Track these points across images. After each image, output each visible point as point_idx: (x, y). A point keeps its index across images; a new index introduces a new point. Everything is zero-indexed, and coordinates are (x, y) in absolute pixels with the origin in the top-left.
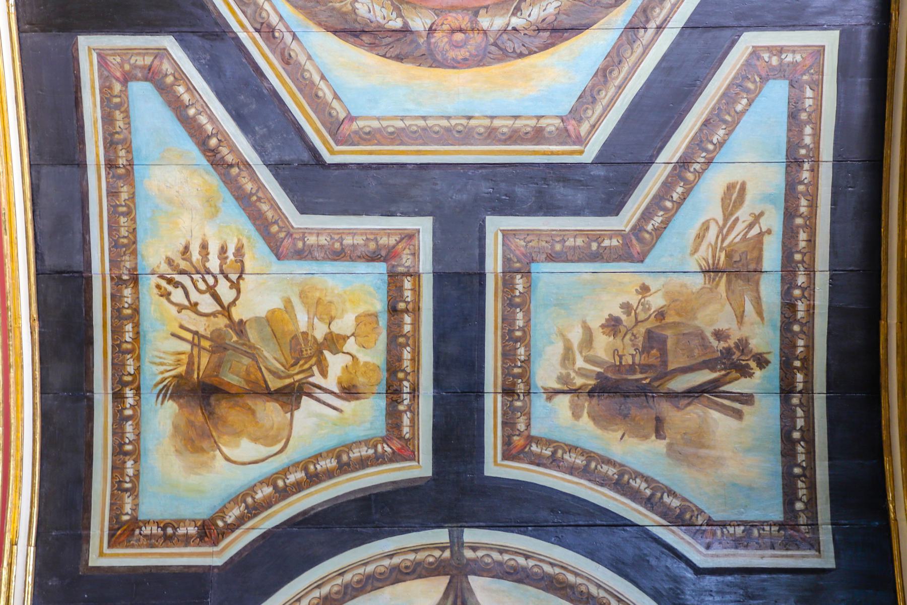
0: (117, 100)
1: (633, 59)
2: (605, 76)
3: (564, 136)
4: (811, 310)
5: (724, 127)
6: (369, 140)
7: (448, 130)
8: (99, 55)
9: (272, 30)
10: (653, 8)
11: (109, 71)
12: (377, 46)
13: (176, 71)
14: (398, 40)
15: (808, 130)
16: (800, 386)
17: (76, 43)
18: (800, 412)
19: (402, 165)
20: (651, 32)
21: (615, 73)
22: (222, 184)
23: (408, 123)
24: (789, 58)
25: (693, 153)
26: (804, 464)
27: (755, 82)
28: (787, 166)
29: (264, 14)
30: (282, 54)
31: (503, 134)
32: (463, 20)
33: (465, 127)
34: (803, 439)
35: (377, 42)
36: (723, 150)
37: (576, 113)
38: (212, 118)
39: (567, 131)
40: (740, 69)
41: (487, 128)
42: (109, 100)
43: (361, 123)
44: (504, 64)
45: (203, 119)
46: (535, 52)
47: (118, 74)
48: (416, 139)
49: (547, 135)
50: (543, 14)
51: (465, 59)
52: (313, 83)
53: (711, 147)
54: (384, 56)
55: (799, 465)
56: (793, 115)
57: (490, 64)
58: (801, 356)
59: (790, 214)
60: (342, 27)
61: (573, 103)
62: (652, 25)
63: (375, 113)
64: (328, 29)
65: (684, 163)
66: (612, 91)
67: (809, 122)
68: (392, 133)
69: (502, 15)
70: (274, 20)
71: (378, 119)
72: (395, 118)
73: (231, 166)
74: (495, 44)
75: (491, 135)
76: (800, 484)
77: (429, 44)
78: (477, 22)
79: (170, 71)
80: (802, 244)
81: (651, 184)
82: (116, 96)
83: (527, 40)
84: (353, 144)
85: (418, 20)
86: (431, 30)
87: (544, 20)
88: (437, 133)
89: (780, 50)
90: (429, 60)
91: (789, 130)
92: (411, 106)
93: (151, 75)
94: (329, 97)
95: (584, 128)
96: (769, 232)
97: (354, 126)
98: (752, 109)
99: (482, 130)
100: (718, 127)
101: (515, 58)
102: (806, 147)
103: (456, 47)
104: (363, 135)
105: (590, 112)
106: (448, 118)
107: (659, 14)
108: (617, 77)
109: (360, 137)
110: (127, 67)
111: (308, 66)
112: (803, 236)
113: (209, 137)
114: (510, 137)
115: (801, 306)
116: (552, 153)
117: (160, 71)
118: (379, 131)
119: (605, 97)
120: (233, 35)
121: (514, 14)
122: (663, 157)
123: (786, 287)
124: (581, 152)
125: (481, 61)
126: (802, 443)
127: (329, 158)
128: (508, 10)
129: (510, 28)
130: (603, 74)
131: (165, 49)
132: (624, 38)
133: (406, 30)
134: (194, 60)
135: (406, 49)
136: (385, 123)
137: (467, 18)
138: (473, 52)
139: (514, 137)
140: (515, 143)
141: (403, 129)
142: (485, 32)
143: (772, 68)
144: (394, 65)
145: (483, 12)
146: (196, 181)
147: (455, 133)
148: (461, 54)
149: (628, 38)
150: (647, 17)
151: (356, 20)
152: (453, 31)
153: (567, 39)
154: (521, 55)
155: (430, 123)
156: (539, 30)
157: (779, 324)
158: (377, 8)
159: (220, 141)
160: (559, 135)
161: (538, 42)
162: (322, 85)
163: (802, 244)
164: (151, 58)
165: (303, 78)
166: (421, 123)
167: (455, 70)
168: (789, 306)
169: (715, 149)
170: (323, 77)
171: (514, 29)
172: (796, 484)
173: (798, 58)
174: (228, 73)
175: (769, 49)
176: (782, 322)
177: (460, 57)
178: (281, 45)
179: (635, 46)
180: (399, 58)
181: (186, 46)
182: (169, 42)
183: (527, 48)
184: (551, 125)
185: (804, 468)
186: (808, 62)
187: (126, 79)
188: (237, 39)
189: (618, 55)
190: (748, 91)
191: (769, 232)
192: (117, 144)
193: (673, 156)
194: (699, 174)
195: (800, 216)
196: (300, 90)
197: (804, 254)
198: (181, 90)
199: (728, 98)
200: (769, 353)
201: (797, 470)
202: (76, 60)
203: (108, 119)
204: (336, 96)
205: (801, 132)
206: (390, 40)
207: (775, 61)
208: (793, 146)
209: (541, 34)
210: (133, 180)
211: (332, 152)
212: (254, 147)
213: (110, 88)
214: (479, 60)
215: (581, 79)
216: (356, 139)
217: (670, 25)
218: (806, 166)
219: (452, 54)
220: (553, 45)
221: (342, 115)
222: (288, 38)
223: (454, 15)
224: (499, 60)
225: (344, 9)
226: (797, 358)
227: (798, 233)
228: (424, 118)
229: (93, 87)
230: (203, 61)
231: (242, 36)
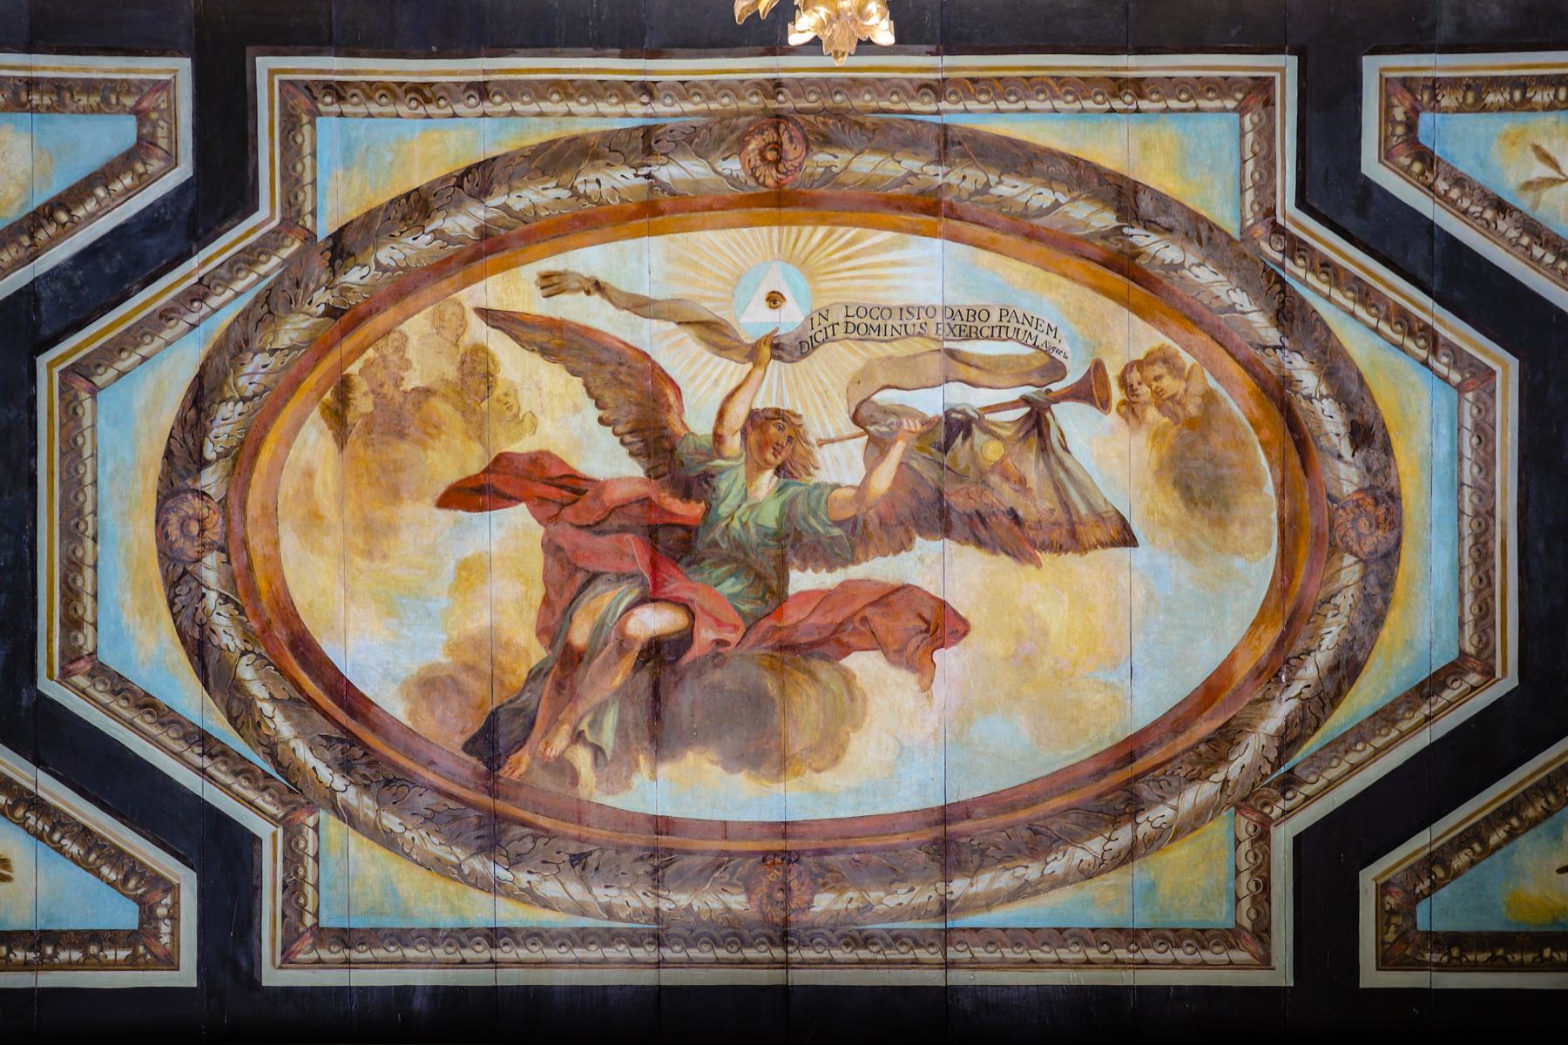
0: (113, 100)
1: (165, 739)
2: (146, 706)
3: (71, 656)
5: (82, 852)
6: (66, 413)
7: (80, 512)
8: (168, 82)
9: (202, 299)
10: (225, 763)
11: (149, 93)
12: (183, 428)
13: (151, 176)
14: (191, 455)
15: (76, 955)
17: (182, 55)
19: (33, 453)
20: (198, 761)
21: (148, 718)
22: (8, 223)
23: (88, 462)
24: (165, 928)
25: (48, 815)
27: (137, 888)
29: (219, 290)
30: (172, 310)
31: (74, 580)
32: (214, 533)
33: (83, 533)
35: (188, 428)
36: (53, 852)
37: (99, 671)
38: (92, 217)
39: (79, 658)
40: (153, 870)
41: (82, 560)
42: (113, 90)
43: (88, 404)
44: (161, 582)
45: (91, 206)
46: (175, 621)
47: (145, 104)
48: (68, 472)
49: (73, 634)
50: (220, 630)
51: (167, 536)
52: (137, 346)
53: (56, 837)
54: (171, 436)
56: (95, 936)
57: (161, 565)
60: (206, 385)
61: (113, 667)
62: (205, 762)
63: (101, 423)
64: (203, 367)
65: (37, 805)
66: (127, 714)
67: (87, 955)
68: (75, 441)
69: (219, 581)
70: (214, 302)
71: (93, 426)
72: (95, 447)
73: (32, 237)
74: (185, 572)
75: (72, 565)
77: (185, 492)
78: (211, 550)
79: (150, 169)
81: (10, 764)
82: (118, 99)
83: (190, 611)
84: (61, 392)
85: (214, 478)
86: (202, 495)
87: (213, 631)
88: (76, 498)
89: (174, 917)
90: (165, 492)
91: (77, 932)
92: (110, 467)
93: (143, 146)
94: (121, 366)
95: (81, 681)
97: (84, 395)
98: (104, 885)
99: (79, 553)
100: (82, 845)
101: (168, 596)
102: (55, 954)
103: (182, 525)
104: (72, 405)
105: (101, 687)
106: (95, 513)
107: (220, 771)
108: (144, 721)
109: (70, 402)
110: (154, 116)
111: (158, 342)
113: (68, 211)
114: (70, 589)
116: (50, 641)
117: (149, 156)
118: (78, 425)
119: (120, 706)
120: (194, 248)
121: (220, 594)
122: (43, 777)
124: (50, 677)
125: (165, 554)
127: (43, 361)
128: (225, 588)
129: (204, 590)
130: (148, 704)
131: (176, 165)
132: (191, 729)
133: (203, 463)
134: (164, 200)
135: (179, 463)
136: (88, 434)
137: (216, 538)
138: (177, 545)
139: (71, 594)
140: (63, 595)
141: (80, 455)
142: (198, 560)
143: (152, 910)
144: (160, 448)
145: (223, 557)
146: (11, 190)
147: (76, 520)
148: (174, 530)
149: (193, 733)
150: (216, 756)
151: (213, 402)
152: (201, 521)
153: (191, 660)
154: (171, 604)
155: (89, 490)
156: (202, 626)
158: (228, 429)
159: (64, 225)
160: (73, 650)
161: (186, 624)
162: (135, 358)
164: (165, 147)
165: (144, 335)
166: (88, 479)
167: (153, 523)
169: (53, 842)
170: (144, 359)
171: (204, 595)
173: (165, 939)
174: (149, 242)
175: (176, 903)
177: (169, 529)
178: (183, 310)
179: (181, 742)
180: (168, 454)
181: (181, 191)
182: (184, 170)
183: (179, 612)
184: (86, 640)
186: (158, 951)
187: (140, 114)
188: (188, 255)
189: (171, 722)
190: (126, 880)
192: (59, 95)
193: (45, 791)
194: (22, 824)
196: (128, 330)
198: (128, 181)
199: (117, 856)
202: (162, 53)
203: (89, 86)
204: (121, 374)
205: (72, 946)
206: (191, 444)
207: (161, 911)
209: (197, 628)
210: (13, 111)
211: (51, 365)
212: (57, 267)
213: (129, 93)
214: (166, 553)
215: (141, 677)
216: (68, 397)
217: (206, 783)
218: (31, 956)
219: (174, 519)
220: (184, 642)
221: (98, 380)
222: (192, 318)
223: (220, 522)
224: (165, 577)
225: (226, 388)
228: (95, 483)
229: (128, 71)
230: (163, 211)
231: (194, 262)
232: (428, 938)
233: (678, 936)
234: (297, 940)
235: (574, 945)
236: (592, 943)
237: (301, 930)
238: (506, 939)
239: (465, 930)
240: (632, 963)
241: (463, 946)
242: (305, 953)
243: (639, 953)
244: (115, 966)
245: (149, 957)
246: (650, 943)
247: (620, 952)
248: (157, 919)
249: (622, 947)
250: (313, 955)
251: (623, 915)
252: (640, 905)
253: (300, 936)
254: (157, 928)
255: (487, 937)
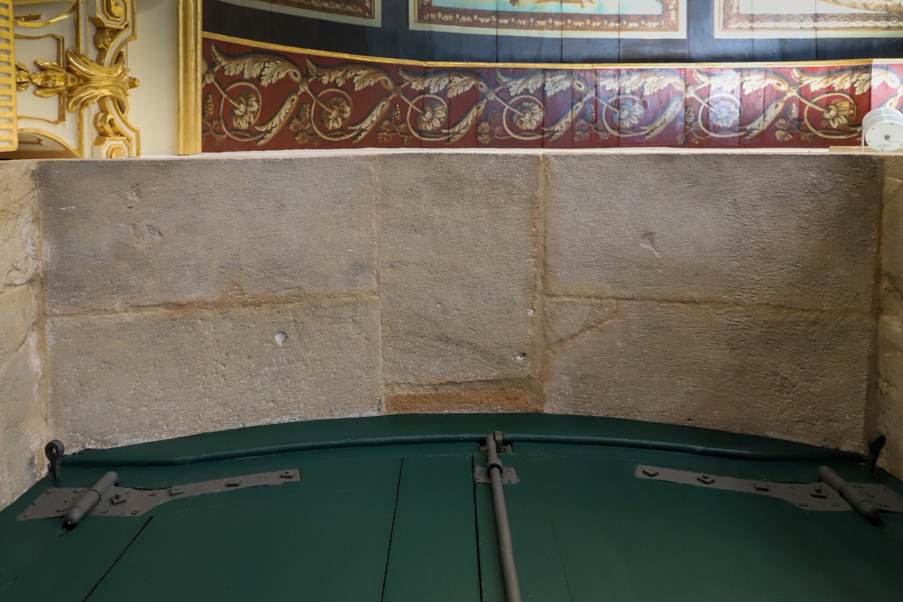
4: (541, 28)
15: (636, 25)
16: (501, 21)
18: (487, 20)
26: (461, 20)
28: (617, 15)
34: (474, 21)
55: (460, 17)
56: (644, 17)
58: (517, 22)
59: (592, 17)
67: (640, 25)
76: (451, 17)
80: (576, 24)
91: (636, 15)
96: (583, 6)
102: (627, 24)
112: (580, 24)
115: (543, 23)
123: (554, 16)
126: (471, 20)
157: (534, 11)
163: (576, 24)
168: (545, 16)
172: (451, 15)
176: (535, 13)
185: (458, 20)
191: (583, 6)
195: (591, 23)
197: (571, 25)
200: (519, 5)
201: (458, 16)
205: (635, 21)
208: (628, 18)
218: (617, 25)
226: (516, 20)
227: (582, 21)
232: (786, 18)
233: (895, 16)
234: (729, 19)
235: (851, 20)
236: (858, 20)
237: (731, 15)
238: (821, 18)
239: (802, 15)
240: (876, 28)
241: (801, 21)
242: (733, 25)
243: (878, 24)
244: (652, 30)
245: (666, 26)
246: (883, 20)
247: (870, 23)
248: (669, 10)
249: (871, 21)
250: (737, 26)
251: (872, 8)
252: (878, 4)
253: (731, 17)
254: (670, 14)
255: (812, 17)
